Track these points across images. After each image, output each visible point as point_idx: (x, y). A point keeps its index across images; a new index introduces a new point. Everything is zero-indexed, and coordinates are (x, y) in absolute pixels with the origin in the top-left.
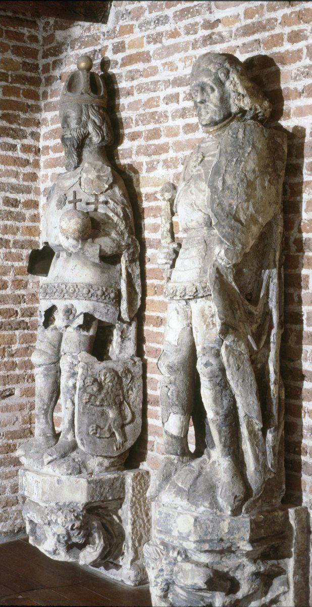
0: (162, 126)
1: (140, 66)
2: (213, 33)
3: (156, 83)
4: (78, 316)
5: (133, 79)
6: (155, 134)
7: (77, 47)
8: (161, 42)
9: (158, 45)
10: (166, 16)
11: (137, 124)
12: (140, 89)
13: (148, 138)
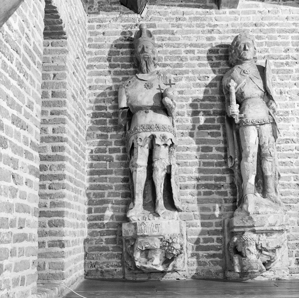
0: (184, 63)
1: (168, 36)
2: (214, 29)
3: (179, 44)
4: (168, 140)
5: (163, 40)
6: (179, 65)
7: (118, 21)
8: (181, 28)
9: (180, 29)
10: (184, 18)
11: (166, 60)
12: (168, 45)
13: (174, 67)
